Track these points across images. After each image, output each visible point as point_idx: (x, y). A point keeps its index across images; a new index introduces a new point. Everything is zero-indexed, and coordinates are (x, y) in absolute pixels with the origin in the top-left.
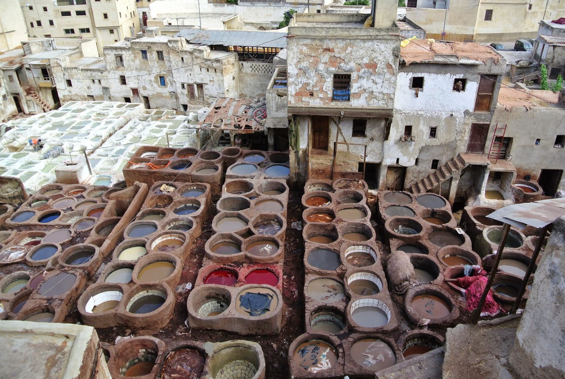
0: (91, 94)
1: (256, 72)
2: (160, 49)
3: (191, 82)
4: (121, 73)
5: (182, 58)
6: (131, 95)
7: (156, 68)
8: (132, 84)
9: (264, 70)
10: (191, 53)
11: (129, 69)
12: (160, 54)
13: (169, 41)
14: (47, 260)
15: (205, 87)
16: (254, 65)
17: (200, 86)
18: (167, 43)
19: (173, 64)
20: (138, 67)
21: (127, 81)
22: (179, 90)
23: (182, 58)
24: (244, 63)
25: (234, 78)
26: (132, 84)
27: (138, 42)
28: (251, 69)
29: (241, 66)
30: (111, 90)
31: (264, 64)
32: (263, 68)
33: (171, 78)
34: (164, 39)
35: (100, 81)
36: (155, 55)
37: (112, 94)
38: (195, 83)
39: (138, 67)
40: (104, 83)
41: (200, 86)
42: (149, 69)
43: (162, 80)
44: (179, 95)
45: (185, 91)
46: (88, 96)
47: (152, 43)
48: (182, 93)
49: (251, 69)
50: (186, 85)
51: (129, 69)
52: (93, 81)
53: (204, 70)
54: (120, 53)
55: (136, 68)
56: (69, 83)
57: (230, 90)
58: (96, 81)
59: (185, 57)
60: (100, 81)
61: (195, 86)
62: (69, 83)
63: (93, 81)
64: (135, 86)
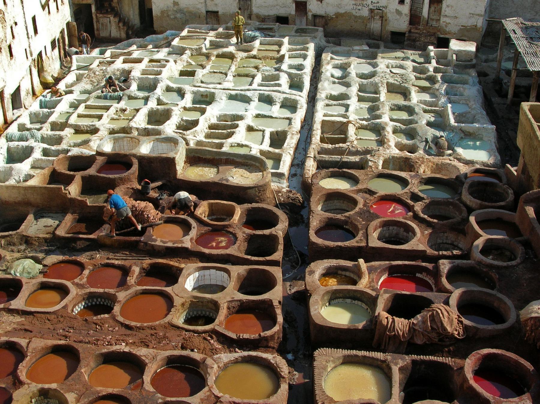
0: (215, 9)
37: (255, 10)
44: (389, 15)
46: (207, 12)
48: (398, 12)
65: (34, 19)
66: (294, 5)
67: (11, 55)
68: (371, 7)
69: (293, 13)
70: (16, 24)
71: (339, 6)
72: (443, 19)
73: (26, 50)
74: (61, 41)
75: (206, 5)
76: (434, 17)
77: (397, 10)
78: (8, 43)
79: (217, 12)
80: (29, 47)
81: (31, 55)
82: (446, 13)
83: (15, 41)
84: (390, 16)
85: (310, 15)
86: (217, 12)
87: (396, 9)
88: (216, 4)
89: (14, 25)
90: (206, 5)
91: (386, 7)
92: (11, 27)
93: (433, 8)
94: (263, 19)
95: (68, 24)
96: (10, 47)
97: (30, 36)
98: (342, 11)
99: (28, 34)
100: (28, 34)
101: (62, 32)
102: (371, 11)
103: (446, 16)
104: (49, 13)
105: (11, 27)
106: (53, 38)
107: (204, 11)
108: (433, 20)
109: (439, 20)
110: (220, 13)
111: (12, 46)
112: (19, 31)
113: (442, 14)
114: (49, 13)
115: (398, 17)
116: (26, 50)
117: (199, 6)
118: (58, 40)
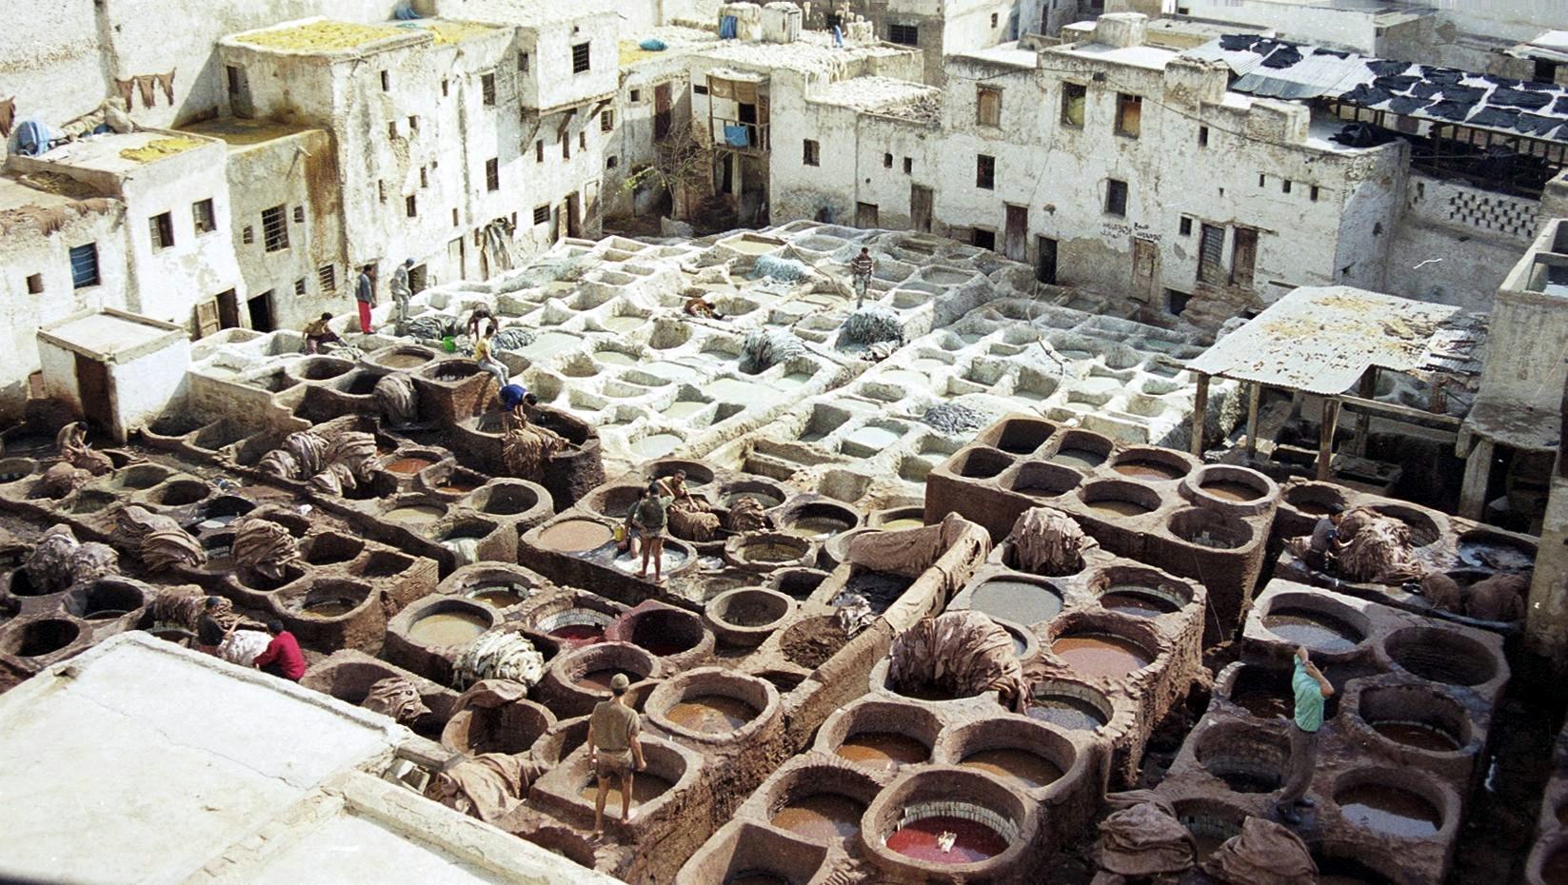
1: (1470, 221)
2: (1132, 85)
3: (1218, 217)
4: (983, 149)
5: (1204, 132)
7: (1102, 152)
8: (1008, 188)
9: (1503, 220)
10: (1240, 115)
11: (1015, 138)
12: (1129, 104)
13: (1170, 66)
14: (766, 628)
15: (1263, 242)
16: (1466, 197)
17: (1247, 238)
18: (1161, 73)
19: (1167, 145)
20: (1045, 138)
22: (1172, 236)
23: (1204, 132)
24: (1429, 184)
25: (1378, 229)
26: (1008, 188)
27: (1063, 56)
28: (1453, 209)
29: (1416, 193)
30: (937, 197)
31: (1505, 198)
32: (1498, 211)
33: (1152, 193)
34: (1158, 59)
35: (908, 163)
36: (1109, 105)
38: (1231, 222)
39: (1045, 138)
40: (919, 175)
41: (1247, 238)
42: (1082, 148)
43: (1116, 196)
45: (1191, 244)
46: (860, 204)
47: (1110, 65)
48: (1179, 252)
49: (1453, 209)
50: (1196, 227)
51: (1015, 138)
52: (889, 160)
53: (1274, 186)
54: (998, 81)
56: (810, 152)
57: (1353, 270)
59: (1218, 124)
60: (908, 163)
62: (810, 152)
63: (889, 160)
65: (492, 167)
67: (412, 211)
68: (1134, 233)
69: (1002, 228)
70: (435, 165)
71: (1082, 225)
72: (1257, 277)
74: (564, 211)
75: (857, 191)
76: (1244, 270)
77: (1177, 247)
78: (407, 192)
81: (470, 221)
83: (429, 192)
84: (1167, 258)
85: (1031, 238)
89: (429, 167)
90: (857, 191)
91: (1157, 238)
92: (423, 170)
93: (1241, 251)
94: (950, 232)
96: (411, 201)
97: (472, 190)
101: (572, 201)
102: (1135, 243)
104: (540, 159)
105: (423, 170)
106: (543, 203)
111: (418, 198)
112: (448, 176)
114: (540, 159)
115: (1178, 261)
117: (846, 191)
118: (557, 210)
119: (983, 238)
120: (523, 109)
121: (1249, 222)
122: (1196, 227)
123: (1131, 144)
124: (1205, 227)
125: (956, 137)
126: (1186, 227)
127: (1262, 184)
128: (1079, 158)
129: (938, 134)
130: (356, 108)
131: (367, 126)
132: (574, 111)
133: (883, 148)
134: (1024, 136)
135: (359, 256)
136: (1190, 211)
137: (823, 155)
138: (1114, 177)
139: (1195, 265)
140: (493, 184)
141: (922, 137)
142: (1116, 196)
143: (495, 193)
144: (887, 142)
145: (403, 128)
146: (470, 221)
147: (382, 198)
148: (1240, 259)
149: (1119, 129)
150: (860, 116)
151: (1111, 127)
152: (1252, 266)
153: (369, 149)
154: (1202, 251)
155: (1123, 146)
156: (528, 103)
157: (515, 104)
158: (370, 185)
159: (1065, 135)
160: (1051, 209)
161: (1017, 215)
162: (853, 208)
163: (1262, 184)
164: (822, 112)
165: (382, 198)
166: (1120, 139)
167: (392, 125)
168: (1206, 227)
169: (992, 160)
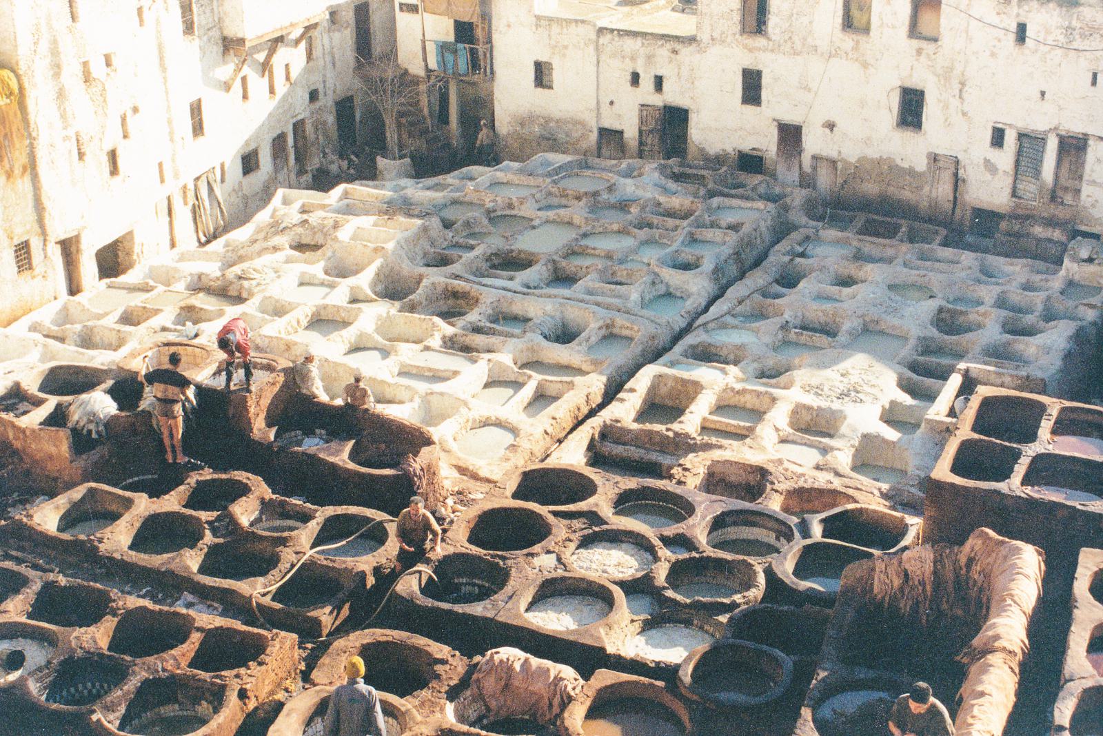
0: (617, 127)
3: (1038, 124)
6: (768, 144)
8: (779, 103)
15: (1095, 151)
17: (1073, 147)
21: (764, 94)
26: (779, 103)
30: (693, 119)
33: (955, 102)
35: (659, 82)
41: (1073, 147)
43: (911, 108)
45: (1005, 158)
48: (990, 166)
50: (1010, 139)
52: (635, 79)
55: (815, 48)
56: (542, 74)
58: (647, 83)
60: (659, 82)
61: (1052, 145)
62: (542, 74)
63: (635, 79)
64: (791, 117)
66: (775, 132)
71: (867, 141)
72: (1086, 190)
73: (160, 165)
75: (599, 115)
76: (1069, 184)
79: (621, 133)
80: (173, 161)
81: (176, 176)
82: (1095, 177)
84: (974, 175)
86: (621, 133)
87: (985, 159)
88: (619, 116)
89: (129, 113)
90: (599, 115)
92: (124, 119)
95: (298, 127)
96: (113, 155)
98: (873, 153)
99: (171, 133)
100: (171, 133)
103: (1094, 182)
104: (245, 97)
105: (124, 119)
107: (593, 125)
108: (1066, 189)
109: (1079, 191)
110: (626, 135)
111: (119, 153)
113: (1086, 177)
114: (245, 97)
115: (988, 177)
116: (160, 165)
119: (750, 162)
120: (224, 39)
121: (1076, 127)
122: (1010, 139)
123: (929, 47)
124: (1022, 136)
125: (716, 50)
126: (998, 138)
127: (1094, 83)
128: (865, 65)
129: (693, 47)
130: (44, 47)
131: (57, 69)
132: (280, 39)
133: (629, 67)
134: (798, 46)
135: (59, 229)
136: (1003, 119)
137: (557, 77)
138: (908, 84)
139: (1010, 180)
140: (198, 129)
141: (675, 52)
142: (911, 108)
143: (201, 139)
144: (633, 59)
145: (98, 69)
146: (176, 176)
147: (81, 155)
148: (1064, 172)
149: (914, 30)
150: (601, 31)
151: (904, 29)
152: (1081, 178)
153: (61, 95)
154: (1017, 163)
155: (919, 52)
156: (232, 31)
157: (215, 33)
158: (66, 138)
159: (847, 41)
160: (831, 126)
161: (790, 135)
162: (594, 136)
163: (1094, 83)
164: (555, 29)
165: (81, 155)
166: (915, 43)
167: (85, 64)
168: (1022, 136)
169: (759, 74)
